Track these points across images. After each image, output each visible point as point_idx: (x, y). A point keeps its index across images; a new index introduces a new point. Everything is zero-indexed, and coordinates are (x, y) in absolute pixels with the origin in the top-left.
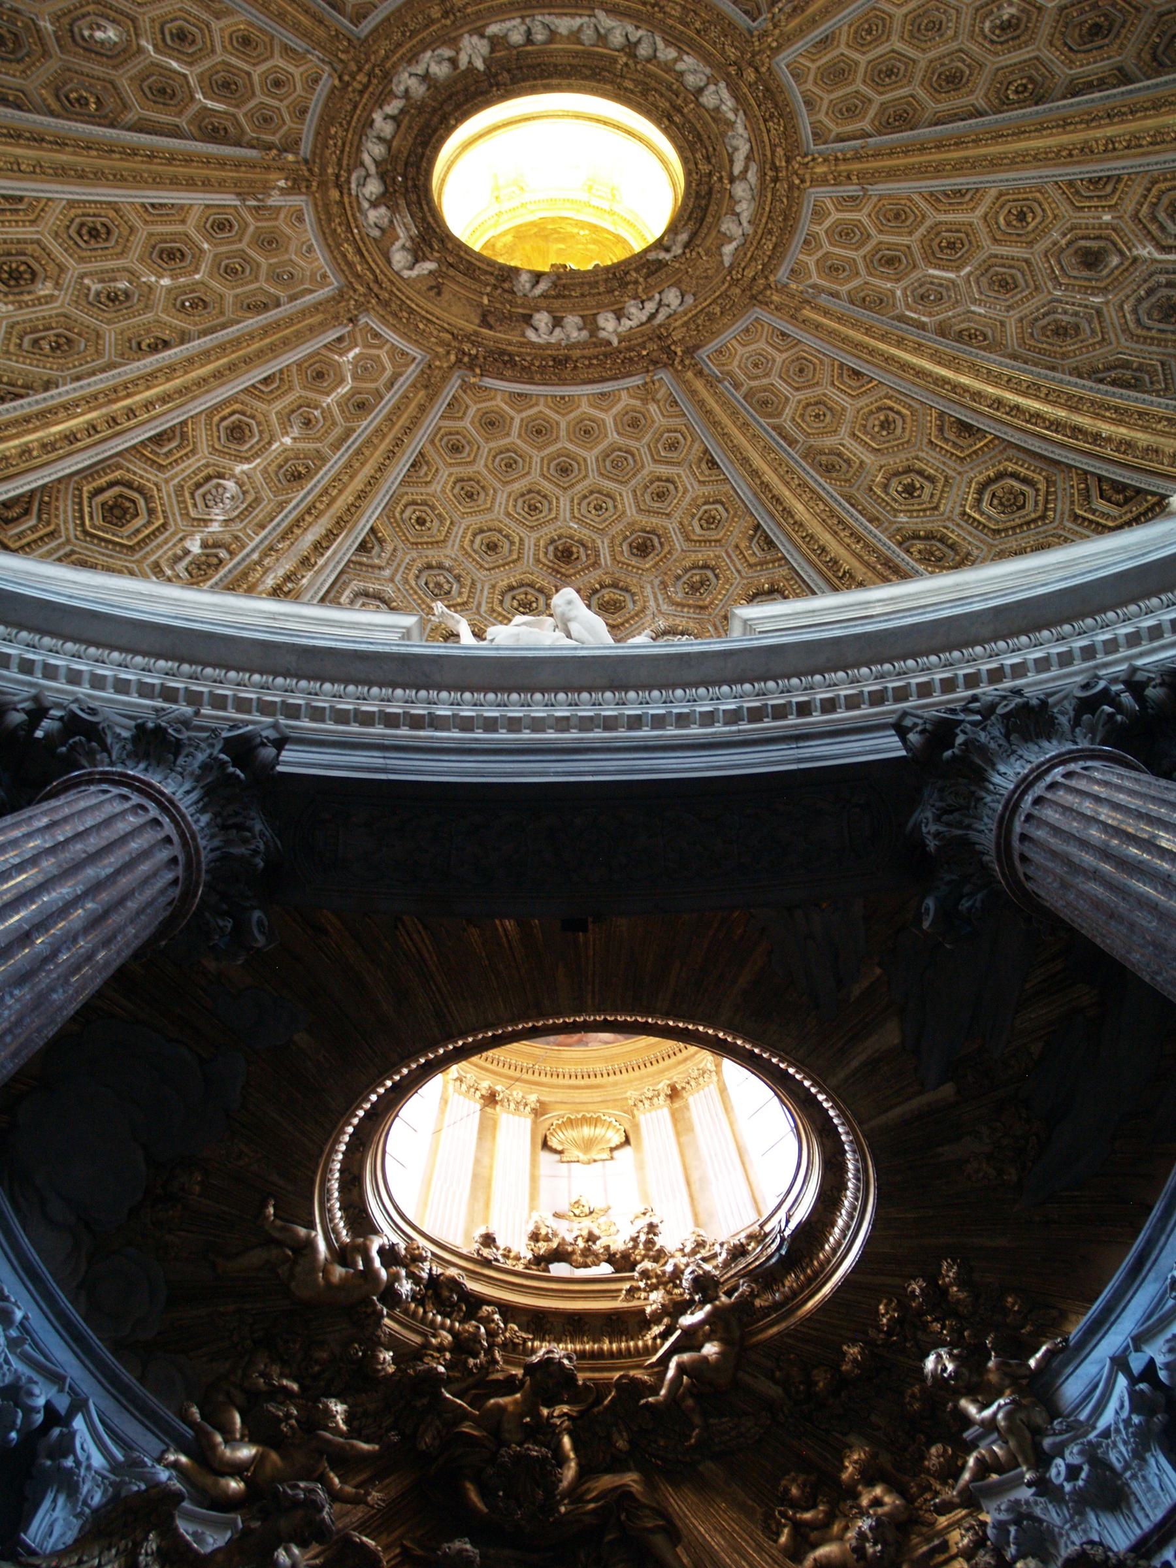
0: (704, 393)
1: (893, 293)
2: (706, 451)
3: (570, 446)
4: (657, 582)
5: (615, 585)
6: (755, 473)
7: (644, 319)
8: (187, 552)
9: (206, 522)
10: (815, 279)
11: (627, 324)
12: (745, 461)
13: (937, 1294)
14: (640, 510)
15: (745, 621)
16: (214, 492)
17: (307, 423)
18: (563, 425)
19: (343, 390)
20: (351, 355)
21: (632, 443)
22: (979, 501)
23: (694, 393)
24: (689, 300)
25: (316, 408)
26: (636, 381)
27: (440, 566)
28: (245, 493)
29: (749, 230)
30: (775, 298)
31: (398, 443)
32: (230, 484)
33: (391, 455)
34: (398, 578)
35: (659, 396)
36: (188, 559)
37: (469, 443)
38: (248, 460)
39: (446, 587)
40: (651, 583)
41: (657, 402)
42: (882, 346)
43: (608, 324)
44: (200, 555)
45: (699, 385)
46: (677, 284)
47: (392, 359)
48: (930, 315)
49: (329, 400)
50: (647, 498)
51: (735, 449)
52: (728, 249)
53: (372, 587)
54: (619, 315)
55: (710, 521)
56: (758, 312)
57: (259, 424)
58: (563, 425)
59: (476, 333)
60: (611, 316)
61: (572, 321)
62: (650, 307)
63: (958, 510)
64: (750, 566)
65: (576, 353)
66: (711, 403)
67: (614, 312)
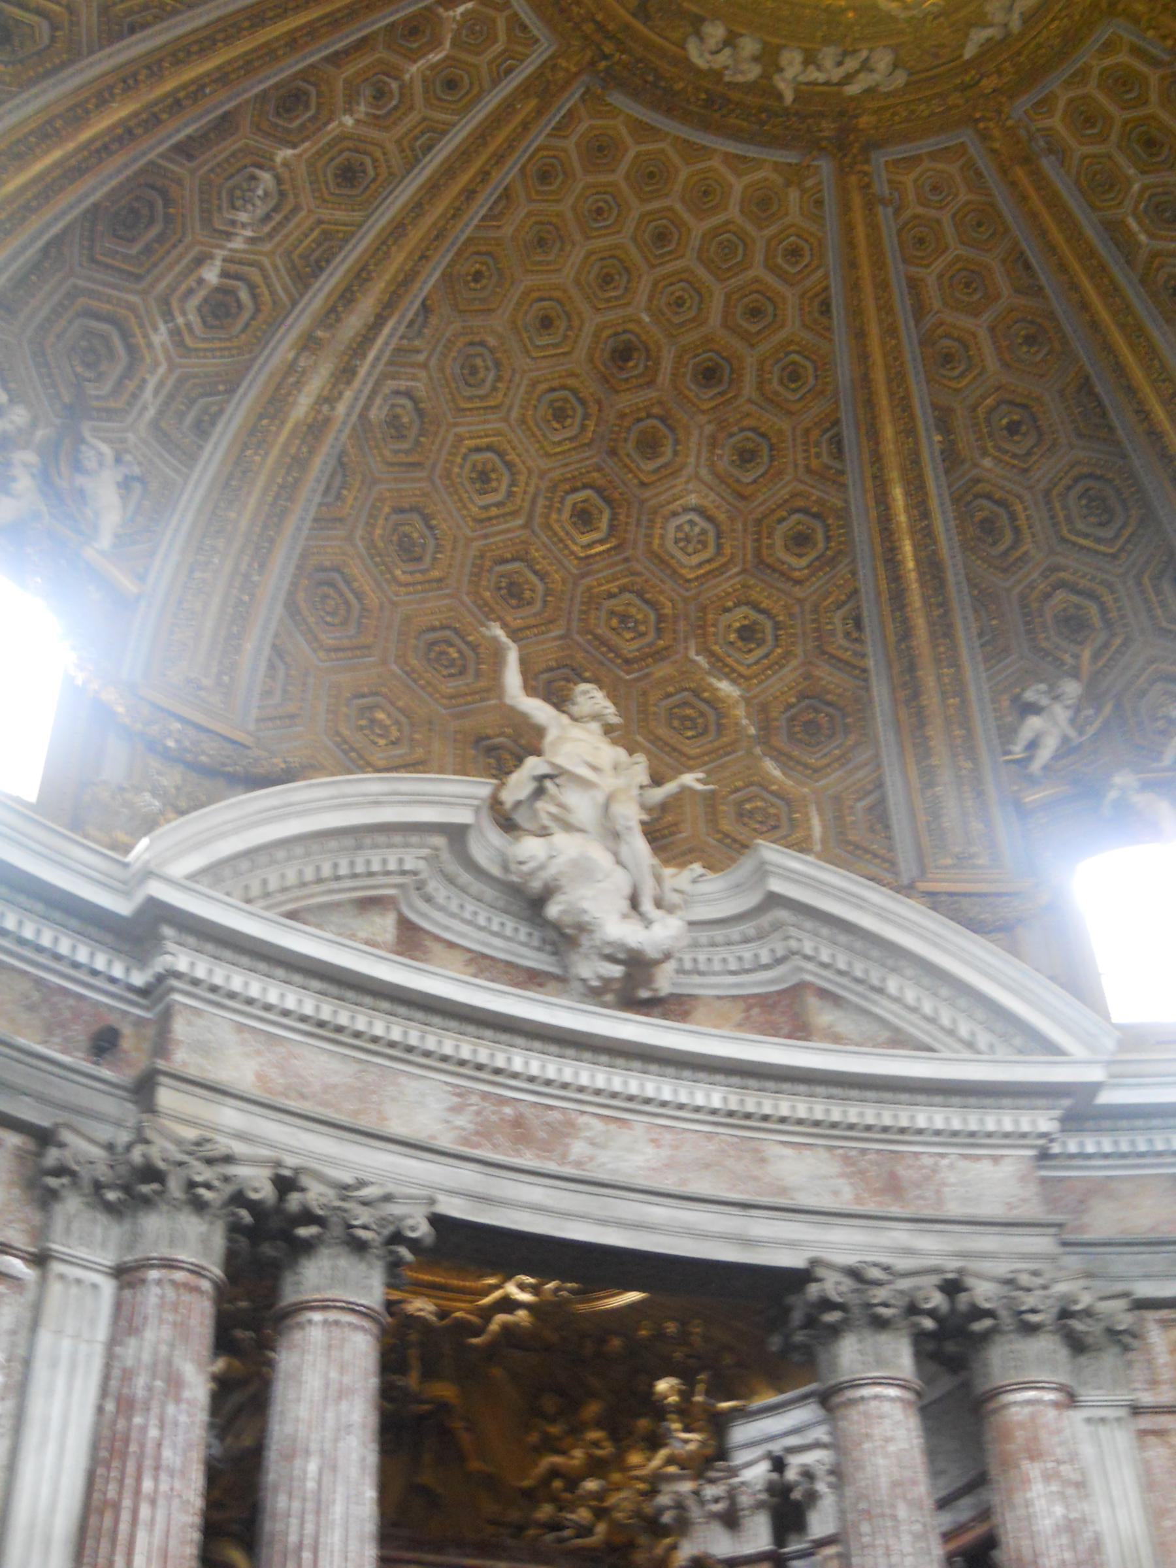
0: (858, 216)
1: (1129, 182)
2: (826, 289)
3: (678, 207)
4: (709, 429)
5: (663, 420)
6: (863, 357)
7: (835, 79)
8: (201, 281)
9: (229, 236)
10: (1056, 122)
11: (814, 75)
12: (860, 335)
13: (683, 1338)
14: (725, 325)
15: (763, 863)
16: (245, 186)
17: (380, 94)
18: (683, 176)
19: (435, 57)
20: (461, 9)
21: (750, 228)
22: (1069, 488)
23: (846, 208)
24: (900, 78)
25: (396, 78)
26: (791, 157)
27: (482, 344)
28: (282, 194)
29: (1016, 25)
30: (996, 133)
31: (484, 175)
32: (266, 177)
33: (470, 194)
34: (433, 363)
35: (809, 183)
36: (202, 293)
37: (565, 173)
38: (294, 146)
39: (481, 374)
40: (701, 427)
41: (803, 191)
42: (1075, 266)
43: (792, 63)
44: (219, 289)
45: (857, 200)
46: (895, 49)
47: (509, 30)
48: (1151, 236)
49: (414, 69)
50: (739, 310)
51: (856, 312)
52: (979, 36)
53: (403, 384)
54: (810, 60)
55: (794, 376)
56: (967, 136)
57: (319, 95)
58: (683, 176)
59: (627, 27)
60: (798, 57)
61: (749, 46)
62: (851, 64)
63: (1043, 485)
64: (809, 470)
65: (736, 96)
66: (861, 232)
67: (806, 51)
